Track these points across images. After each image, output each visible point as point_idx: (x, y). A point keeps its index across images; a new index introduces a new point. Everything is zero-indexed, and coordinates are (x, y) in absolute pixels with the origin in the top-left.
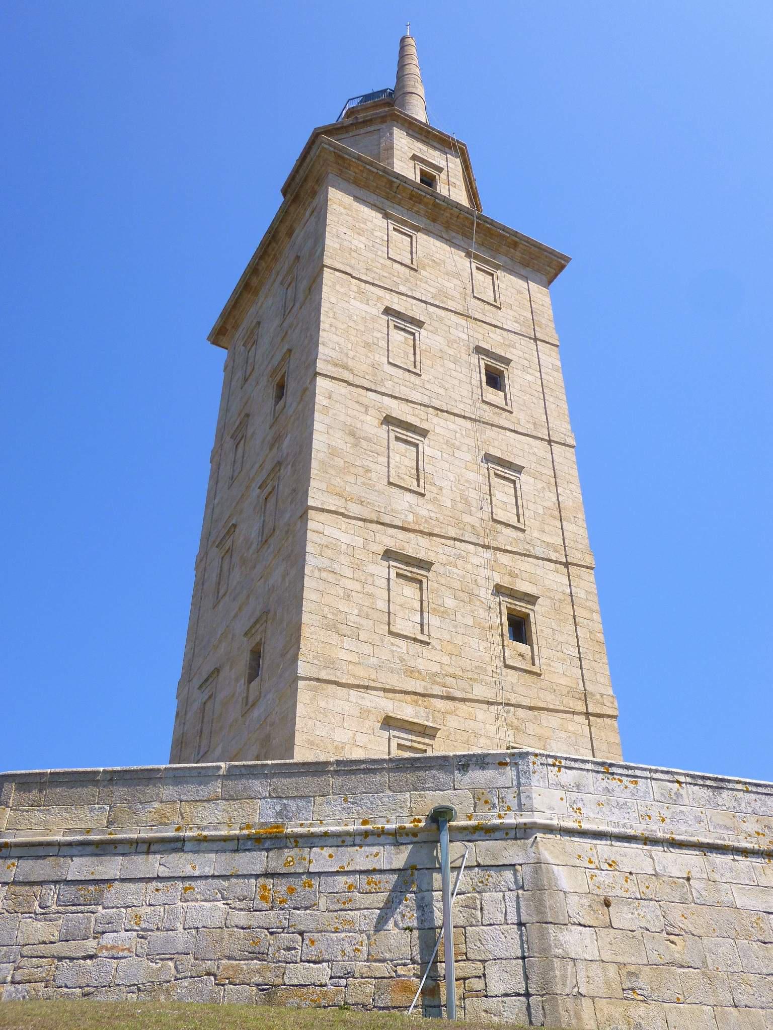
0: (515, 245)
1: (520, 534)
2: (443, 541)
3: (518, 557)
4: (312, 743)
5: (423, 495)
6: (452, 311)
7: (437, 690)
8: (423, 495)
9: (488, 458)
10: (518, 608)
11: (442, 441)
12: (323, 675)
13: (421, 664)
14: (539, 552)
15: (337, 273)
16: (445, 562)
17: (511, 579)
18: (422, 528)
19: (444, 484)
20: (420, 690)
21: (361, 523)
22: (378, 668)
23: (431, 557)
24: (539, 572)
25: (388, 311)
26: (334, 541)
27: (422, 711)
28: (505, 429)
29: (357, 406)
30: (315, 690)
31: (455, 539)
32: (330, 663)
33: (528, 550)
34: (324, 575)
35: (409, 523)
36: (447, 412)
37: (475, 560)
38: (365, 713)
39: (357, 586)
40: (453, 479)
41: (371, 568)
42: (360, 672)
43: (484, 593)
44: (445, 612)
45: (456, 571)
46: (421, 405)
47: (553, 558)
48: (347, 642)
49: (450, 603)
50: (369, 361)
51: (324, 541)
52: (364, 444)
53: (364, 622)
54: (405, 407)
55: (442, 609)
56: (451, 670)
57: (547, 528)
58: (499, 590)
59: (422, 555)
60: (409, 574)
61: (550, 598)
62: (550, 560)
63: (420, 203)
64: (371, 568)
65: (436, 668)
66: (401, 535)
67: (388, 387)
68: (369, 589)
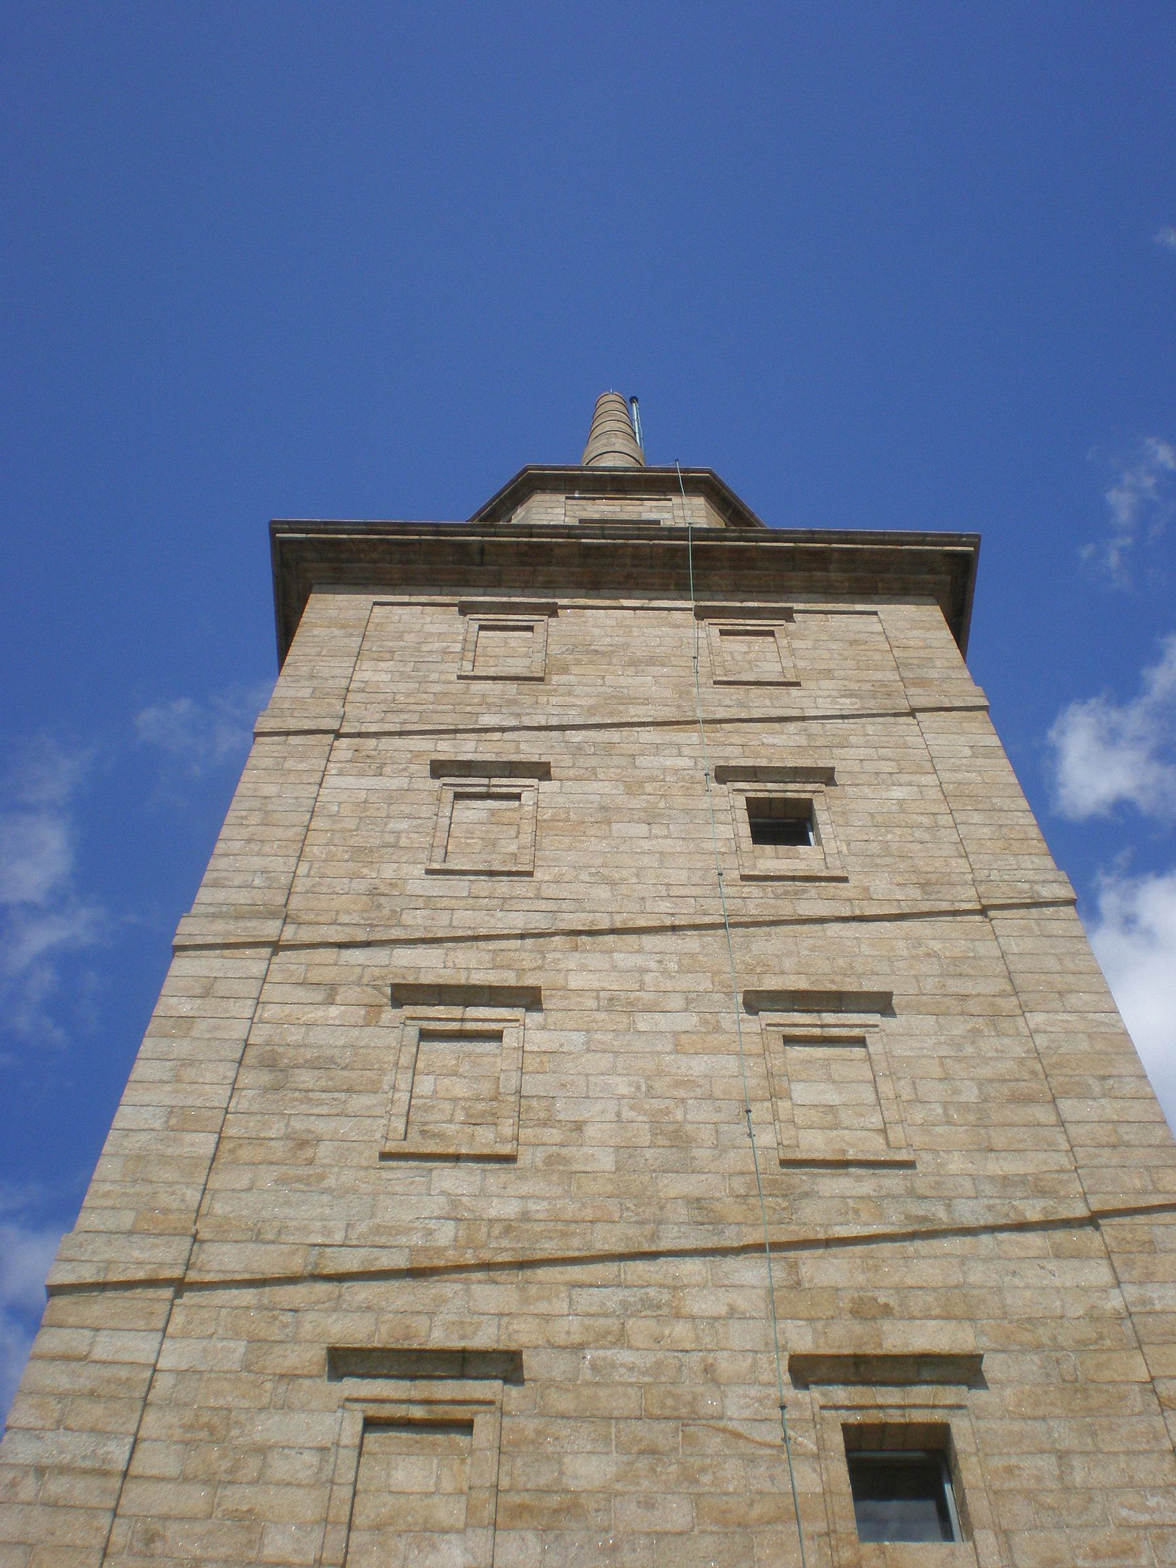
1: (893, 1181)
2: (575, 1273)
3: (887, 1248)
8: (510, 1159)
9: (755, 1002)
11: (593, 1004)
14: (968, 1212)
15: (292, 740)
16: (576, 1338)
17: (858, 1328)
18: (486, 1256)
21: (248, 1296)
23: (522, 1334)
25: (439, 769)
26: (123, 1373)
28: (821, 920)
29: (300, 994)
34: (56, 1487)
35: (440, 1251)
36: (613, 931)
39: (196, 1498)
40: (624, 1090)
45: (625, 1356)
46: (522, 936)
47: (1033, 1215)
49: (588, 1468)
50: (361, 886)
51: (86, 1378)
52: (306, 1078)
55: (554, 1501)
57: (999, 1138)
58: (805, 1370)
59: (484, 1338)
60: (418, 1412)
61: (1039, 1347)
62: (1023, 1227)
63: (549, 563)
66: (400, 1295)
67: (417, 921)
68: (238, 1497)
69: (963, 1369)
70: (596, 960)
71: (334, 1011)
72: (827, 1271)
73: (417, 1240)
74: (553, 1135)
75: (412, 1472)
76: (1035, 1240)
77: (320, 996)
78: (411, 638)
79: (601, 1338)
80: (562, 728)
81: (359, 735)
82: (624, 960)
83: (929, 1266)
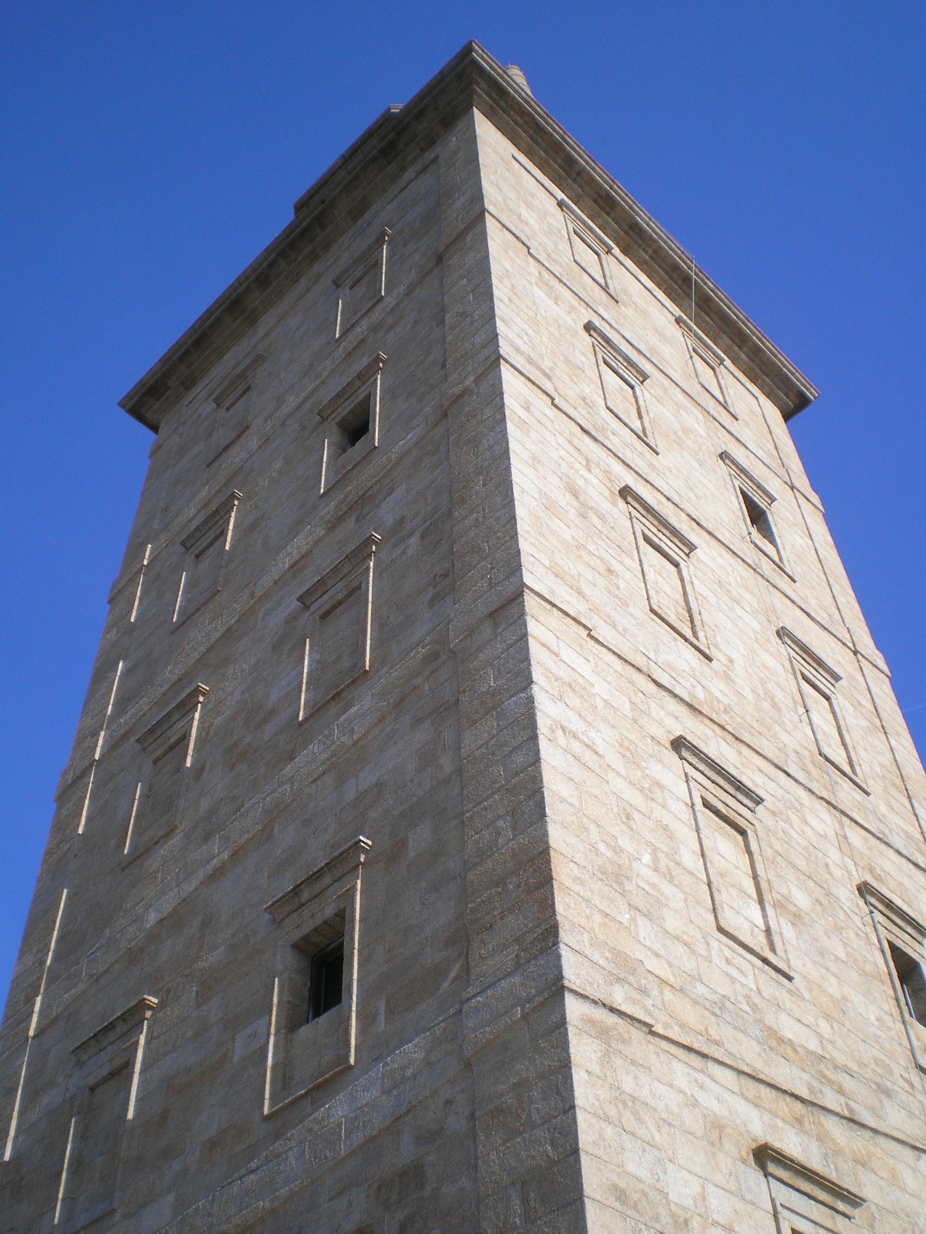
4: (621, 1196)
7: (830, 1100)
12: (619, 997)
13: (789, 1030)
19: (734, 655)
20: (804, 1093)
22: (718, 1007)
27: (814, 1146)
30: (603, 1033)
32: (624, 968)
38: (716, 1131)
39: (638, 800)
41: (656, 770)
42: (691, 1016)
43: (847, 896)
48: (644, 929)
53: (668, 889)
56: (840, 1059)
64: (656, 770)
65: (813, 1045)
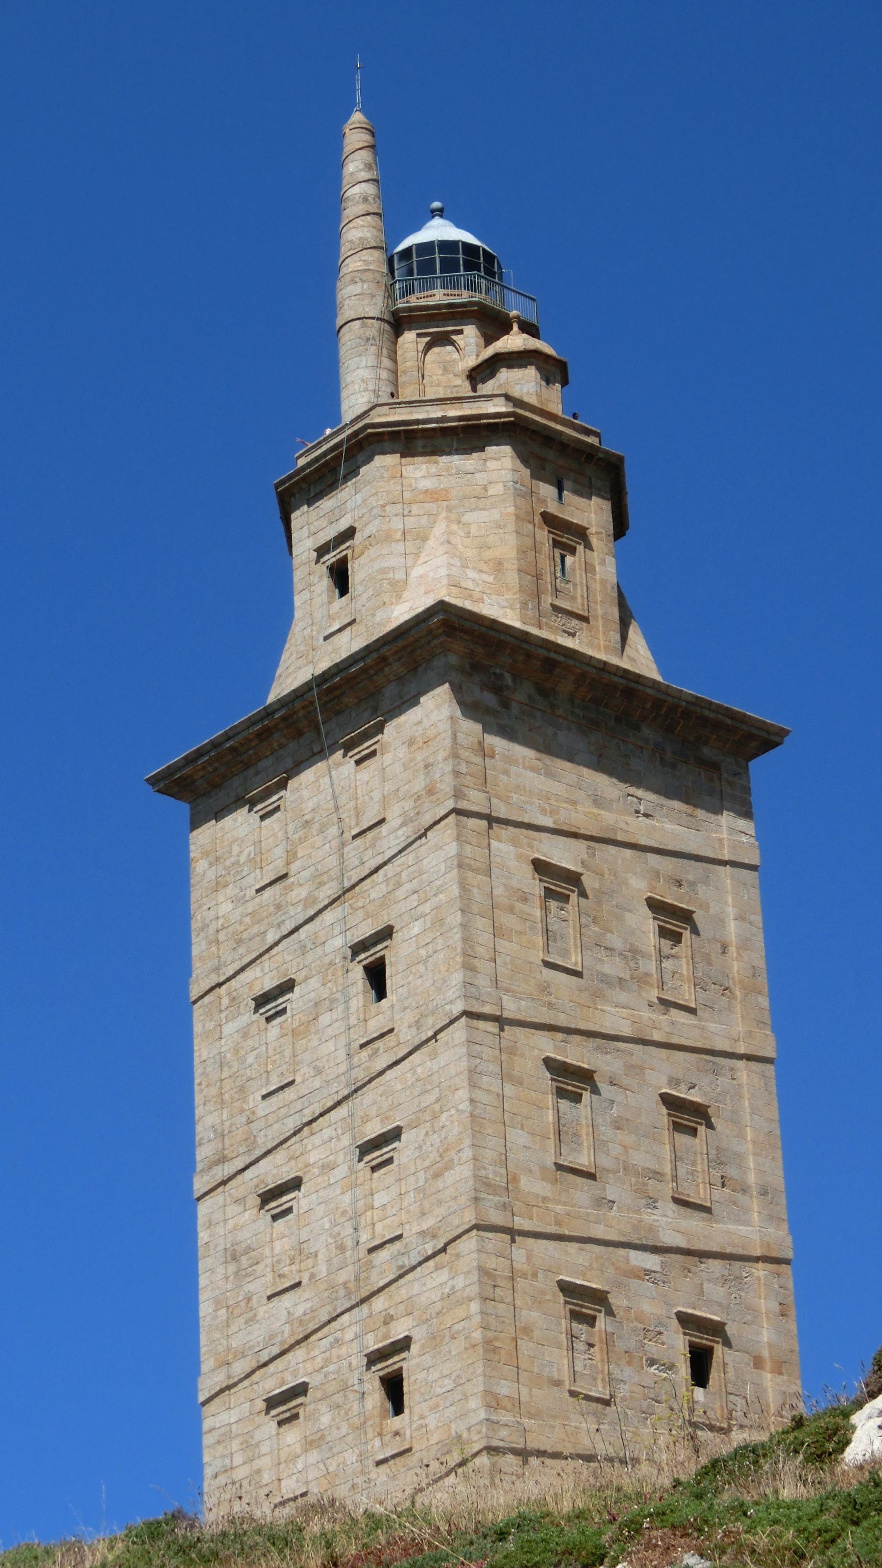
0: (383, 660)
1: (398, 1245)
5: (298, 1284)
6: (326, 907)
10: (390, 1370)
24: (416, 1289)
31: (329, 1322)
33: (402, 1267)
37: (349, 1335)
44: (322, 1437)
45: (332, 1368)
47: (430, 1252)
50: (244, 1120)
54: (279, 1156)
55: (319, 1434)
69: (404, 1344)
70: (316, 1140)
71: (247, 1215)
72: (379, 1303)
73: (279, 1338)
74: (310, 1262)
75: (292, 1435)
76: (431, 1263)
77: (241, 1209)
78: (236, 849)
79: (327, 1362)
80: (296, 929)
81: (229, 979)
82: (327, 1133)
83: (402, 1290)
